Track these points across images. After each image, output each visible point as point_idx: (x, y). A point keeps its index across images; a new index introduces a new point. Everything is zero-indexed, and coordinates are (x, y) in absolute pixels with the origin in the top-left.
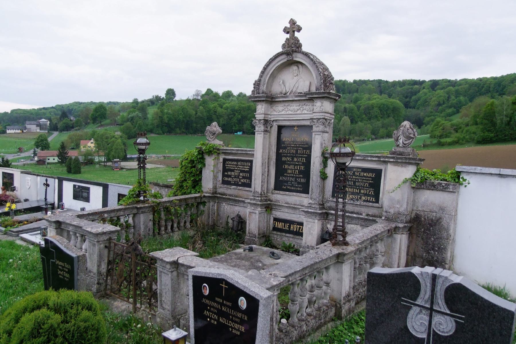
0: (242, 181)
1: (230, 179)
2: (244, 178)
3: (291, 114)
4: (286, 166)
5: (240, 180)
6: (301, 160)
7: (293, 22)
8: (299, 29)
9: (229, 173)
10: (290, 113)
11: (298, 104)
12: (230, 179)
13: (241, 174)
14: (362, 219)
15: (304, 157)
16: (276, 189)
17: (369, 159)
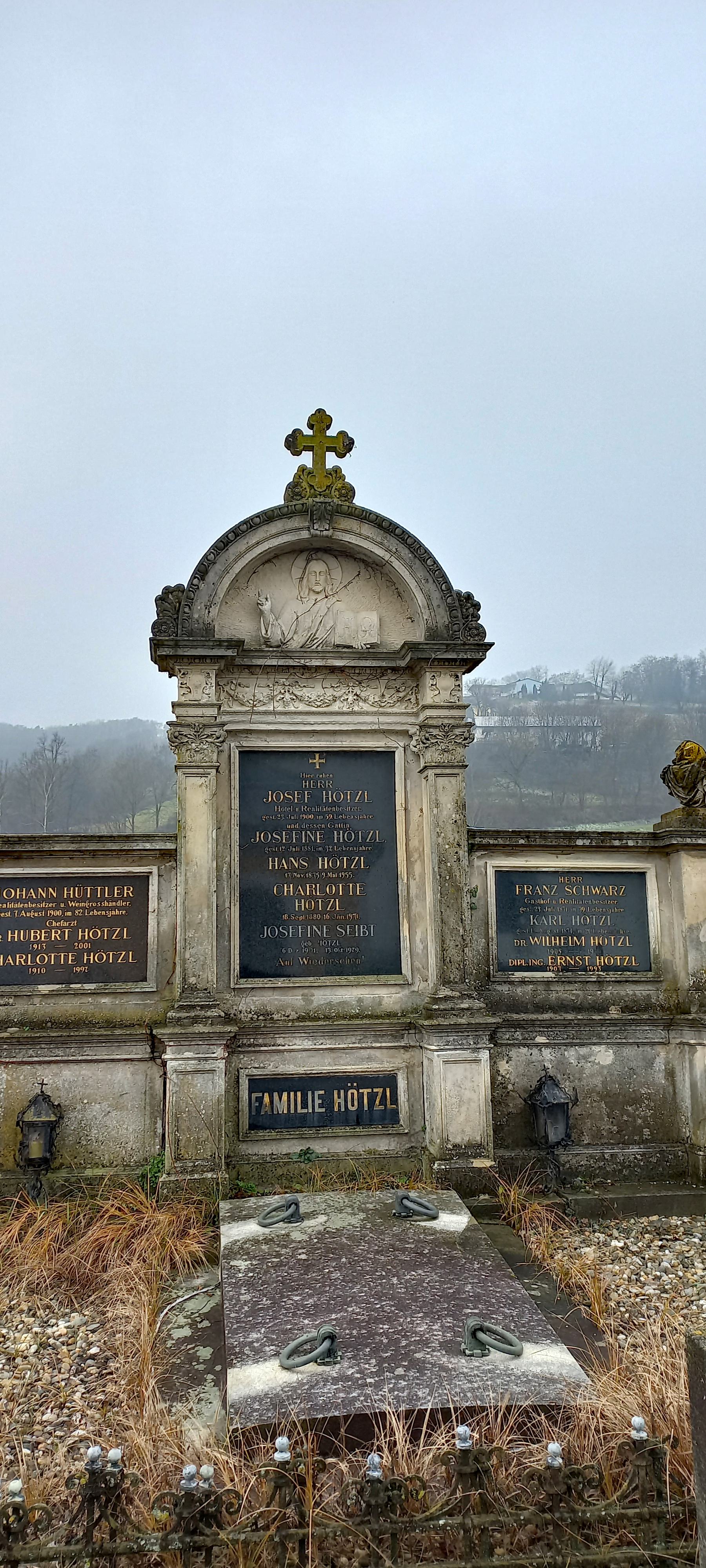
1: (20, 960)
2: (96, 945)
4: (288, 889)
8: (344, 445)
10: (302, 707)
11: (332, 680)
12: (20, 960)
13: (88, 934)
14: (614, 1023)
16: (246, 972)
17: (617, 843)
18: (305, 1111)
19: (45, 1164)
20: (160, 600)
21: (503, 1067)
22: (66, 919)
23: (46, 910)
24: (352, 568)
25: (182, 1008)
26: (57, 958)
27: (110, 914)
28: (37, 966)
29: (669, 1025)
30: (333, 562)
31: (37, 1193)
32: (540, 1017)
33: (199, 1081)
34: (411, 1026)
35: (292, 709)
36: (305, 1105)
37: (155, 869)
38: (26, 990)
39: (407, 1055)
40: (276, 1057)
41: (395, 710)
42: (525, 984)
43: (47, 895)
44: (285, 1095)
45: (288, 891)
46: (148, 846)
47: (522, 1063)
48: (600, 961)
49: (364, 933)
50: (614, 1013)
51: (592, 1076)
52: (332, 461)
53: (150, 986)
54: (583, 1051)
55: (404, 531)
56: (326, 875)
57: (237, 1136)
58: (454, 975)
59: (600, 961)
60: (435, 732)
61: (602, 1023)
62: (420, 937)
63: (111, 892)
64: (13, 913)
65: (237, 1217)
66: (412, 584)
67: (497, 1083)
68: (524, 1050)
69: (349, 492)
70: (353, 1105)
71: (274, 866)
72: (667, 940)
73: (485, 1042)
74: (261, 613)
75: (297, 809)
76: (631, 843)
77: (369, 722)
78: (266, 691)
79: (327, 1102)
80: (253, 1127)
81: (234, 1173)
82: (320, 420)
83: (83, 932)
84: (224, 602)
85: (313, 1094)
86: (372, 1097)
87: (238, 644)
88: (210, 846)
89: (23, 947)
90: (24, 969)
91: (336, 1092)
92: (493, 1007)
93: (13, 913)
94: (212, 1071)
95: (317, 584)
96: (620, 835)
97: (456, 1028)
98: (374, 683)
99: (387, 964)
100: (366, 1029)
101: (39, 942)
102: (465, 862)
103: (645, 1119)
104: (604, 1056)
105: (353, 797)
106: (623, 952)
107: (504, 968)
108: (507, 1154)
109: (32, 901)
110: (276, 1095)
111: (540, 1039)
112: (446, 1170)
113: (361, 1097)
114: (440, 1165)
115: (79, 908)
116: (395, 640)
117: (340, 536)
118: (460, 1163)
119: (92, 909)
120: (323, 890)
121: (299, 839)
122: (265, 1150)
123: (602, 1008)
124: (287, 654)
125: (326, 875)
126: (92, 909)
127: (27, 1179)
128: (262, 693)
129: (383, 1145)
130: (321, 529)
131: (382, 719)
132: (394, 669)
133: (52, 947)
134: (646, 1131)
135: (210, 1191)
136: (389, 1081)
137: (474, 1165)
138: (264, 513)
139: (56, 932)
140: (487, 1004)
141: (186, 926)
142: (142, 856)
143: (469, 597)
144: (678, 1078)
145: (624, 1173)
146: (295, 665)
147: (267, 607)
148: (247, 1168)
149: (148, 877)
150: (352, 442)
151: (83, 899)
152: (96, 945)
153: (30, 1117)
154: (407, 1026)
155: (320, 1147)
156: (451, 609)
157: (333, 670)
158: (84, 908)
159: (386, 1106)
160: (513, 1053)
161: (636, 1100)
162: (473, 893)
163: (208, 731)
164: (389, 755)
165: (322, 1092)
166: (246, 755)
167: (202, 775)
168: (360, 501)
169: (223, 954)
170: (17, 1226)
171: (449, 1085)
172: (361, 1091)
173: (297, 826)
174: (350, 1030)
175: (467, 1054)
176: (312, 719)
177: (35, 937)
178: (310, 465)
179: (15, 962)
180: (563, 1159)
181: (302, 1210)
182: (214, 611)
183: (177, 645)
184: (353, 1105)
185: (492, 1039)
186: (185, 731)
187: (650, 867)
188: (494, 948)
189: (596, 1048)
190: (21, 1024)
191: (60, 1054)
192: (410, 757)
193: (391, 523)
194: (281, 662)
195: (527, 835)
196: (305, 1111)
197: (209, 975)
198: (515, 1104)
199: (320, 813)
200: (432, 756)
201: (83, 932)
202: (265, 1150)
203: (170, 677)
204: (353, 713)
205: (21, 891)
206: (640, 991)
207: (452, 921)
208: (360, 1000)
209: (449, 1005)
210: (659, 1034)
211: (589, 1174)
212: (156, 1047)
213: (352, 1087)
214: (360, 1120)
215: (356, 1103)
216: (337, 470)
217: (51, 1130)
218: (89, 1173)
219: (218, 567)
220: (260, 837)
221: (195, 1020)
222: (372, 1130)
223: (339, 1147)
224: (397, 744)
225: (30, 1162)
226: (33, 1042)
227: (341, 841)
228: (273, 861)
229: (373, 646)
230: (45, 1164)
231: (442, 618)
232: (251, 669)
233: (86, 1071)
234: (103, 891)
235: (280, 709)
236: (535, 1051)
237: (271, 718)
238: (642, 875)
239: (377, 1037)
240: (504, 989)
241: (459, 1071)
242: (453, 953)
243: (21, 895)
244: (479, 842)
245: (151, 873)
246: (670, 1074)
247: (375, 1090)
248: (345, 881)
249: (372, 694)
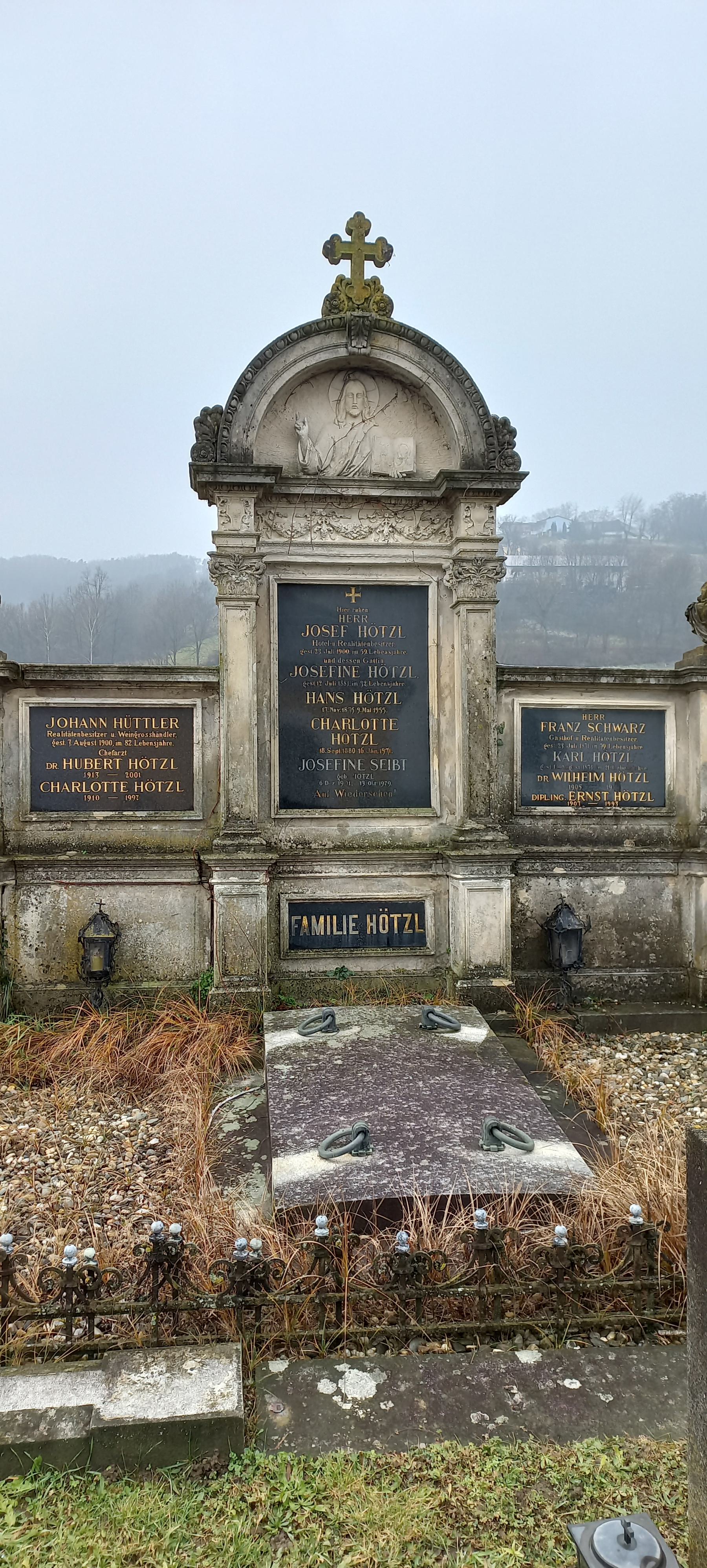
0: (143, 787)
3: (344, 545)
5: (129, 788)
6: (383, 697)
7: (359, 225)
8: (383, 253)
9: (68, 764)
10: (338, 539)
11: (369, 511)
13: (137, 764)
14: (627, 855)
15: (393, 690)
16: (285, 803)
17: (639, 681)
18: (340, 933)
19: (105, 977)
20: (199, 423)
21: (523, 895)
22: (118, 749)
23: (98, 740)
24: (389, 390)
25: (226, 836)
26: (110, 786)
27: (157, 745)
28: (92, 794)
29: (678, 858)
30: (370, 383)
31: (99, 1003)
32: (559, 849)
33: (244, 904)
34: (439, 857)
35: (329, 540)
36: (340, 928)
37: (198, 702)
38: (82, 816)
39: (434, 884)
40: (314, 884)
41: (429, 543)
42: (544, 818)
43: (98, 725)
44: (322, 918)
45: (325, 726)
46: (192, 678)
47: (539, 893)
48: (618, 797)
49: (396, 767)
50: (628, 846)
51: (605, 904)
52: (370, 270)
53: (197, 815)
54: (598, 881)
55: (443, 350)
56: (361, 710)
57: (278, 954)
58: (480, 808)
59: (618, 797)
60: (467, 566)
61: (617, 855)
62: (448, 773)
63: (158, 723)
64: (67, 742)
65: (279, 1027)
66: (449, 408)
67: (516, 910)
68: (542, 880)
69: (387, 305)
70: (384, 929)
71: (311, 700)
72: (681, 778)
73: (507, 872)
74: (298, 438)
75: (334, 644)
76: (653, 681)
77: (402, 555)
78: (303, 522)
79: (361, 925)
80: (292, 947)
81: (276, 988)
82: (359, 225)
83: (133, 762)
84: (262, 426)
85: (348, 918)
86: (402, 922)
87: (274, 471)
88: (251, 679)
89: (78, 775)
90: (79, 796)
91: (368, 917)
92: (516, 839)
93: (67, 742)
94: (255, 895)
95: (354, 407)
96: (643, 674)
97: (482, 859)
98: (408, 515)
99: (416, 796)
100: (399, 858)
101: (93, 771)
102: (493, 699)
103: (651, 944)
104: (617, 886)
105: (387, 632)
106: (640, 788)
107: (527, 802)
108: (524, 975)
109: (83, 729)
110: (314, 918)
111: (558, 870)
112: (468, 989)
113: (391, 921)
114: (462, 983)
115: (128, 738)
116: (431, 468)
117: (378, 355)
118: (482, 982)
119: (140, 740)
120: (358, 725)
121: (335, 674)
122: (304, 967)
123: (617, 841)
124: (323, 483)
125: (361, 710)
126: (140, 740)
127: (88, 990)
128: (299, 523)
129: (412, 965)
130: (360, 346)
131: (417, 552)
132: (429, 500)
133: (105, 775)
134: (652, 956)
135: (256, 1003)
136: (417, 907)
137: (494, 984)
138: (302, 328)
139: (108, 762)
140: (509, 837)
141: (229, 757)
142: (186, 689)
143: (505, 422)
144: (685, 908)
145: (629, 994)
146: (332, 494)
147: (304, 431)
148: (287, 984)
149: (193, 709)
150: (390, 250)
151: (132, 730)
152: (146, 775)
153: (90, 933)
154: (435, 857)
155: (353, 966)
156: (488, 435)
157: (369, 500)
158: (133, 739)
159: (414, 930)
160: (533, 882)
161: (644, 927)
162: (500, 729)
163: (247, 563)
164: (422, 590)
165: (356, 916)
166: (283, 587)
167: (245, 608)
168: (398, 316)
169: (264, 786)
170: (81, 1032)
171: (473, 911)
172: (392, 916)
173: (334, 661)
174: (381, 859)
175: (489, 883)
176: (348, 552)
177: (89, 766)
178: (348, 275)
179: (70, 788)
180: (575, 980)
181: (338, 1022)
182: (253, 435)
183: (216, 471)
184: (384, 929)
185: (514, 869)
186: (225, 562)
187: (669, 706)
188: (518, 783)
189: (609, 879)
190: (79, 848)
191: (116, 876)
192: (443, 592)
193: (430, 340)
194: (319, 491)
195: (554, 672)
196: (340, 933)
197: (251, 806)
198: (532, 930)
199: (355, 648)
200: (464, 591)
201: (133, 762)
202: (304, 967)
203: (210, 506)
204: (387, 546)
205: (74, 720)
206: (653, 826)
207: (479, 755)
208: (392, 831)
209: (474, 837)
210: (669, 866)
211: (598, 994)
212: (203, 872)
213: (383, 912)
214: (390, 942)
215: (387, 927)
216: (375, 281)
217: (110, 946)
218: (145, 985)
219: (256, 387)
220: (298, 671)
221: (239, 848)
222: (401, 951)
223: (371, 966)
224: (429, 578)
225: (92, 975)
226: (90, 865)
227: (376, 676)
228: (311, 696)
229: (409, 475)
230: (105, 977)
231: (479, 446)
232: (289, 498)
233: (140, 893)
234: (150, 723)
235: (317, 540)
236: (553, 881)
237: (308, 550)
238: (661, 714)
239: (408, 866)
240: (527, 823)
241: (481, 899)
242: (479, 787)
243: (74, 725)
244: (508, 679)
245: (195, 705)
246: (678, 904)
247: (404, 915)
248: (379, 716)
249: (407, 526)
